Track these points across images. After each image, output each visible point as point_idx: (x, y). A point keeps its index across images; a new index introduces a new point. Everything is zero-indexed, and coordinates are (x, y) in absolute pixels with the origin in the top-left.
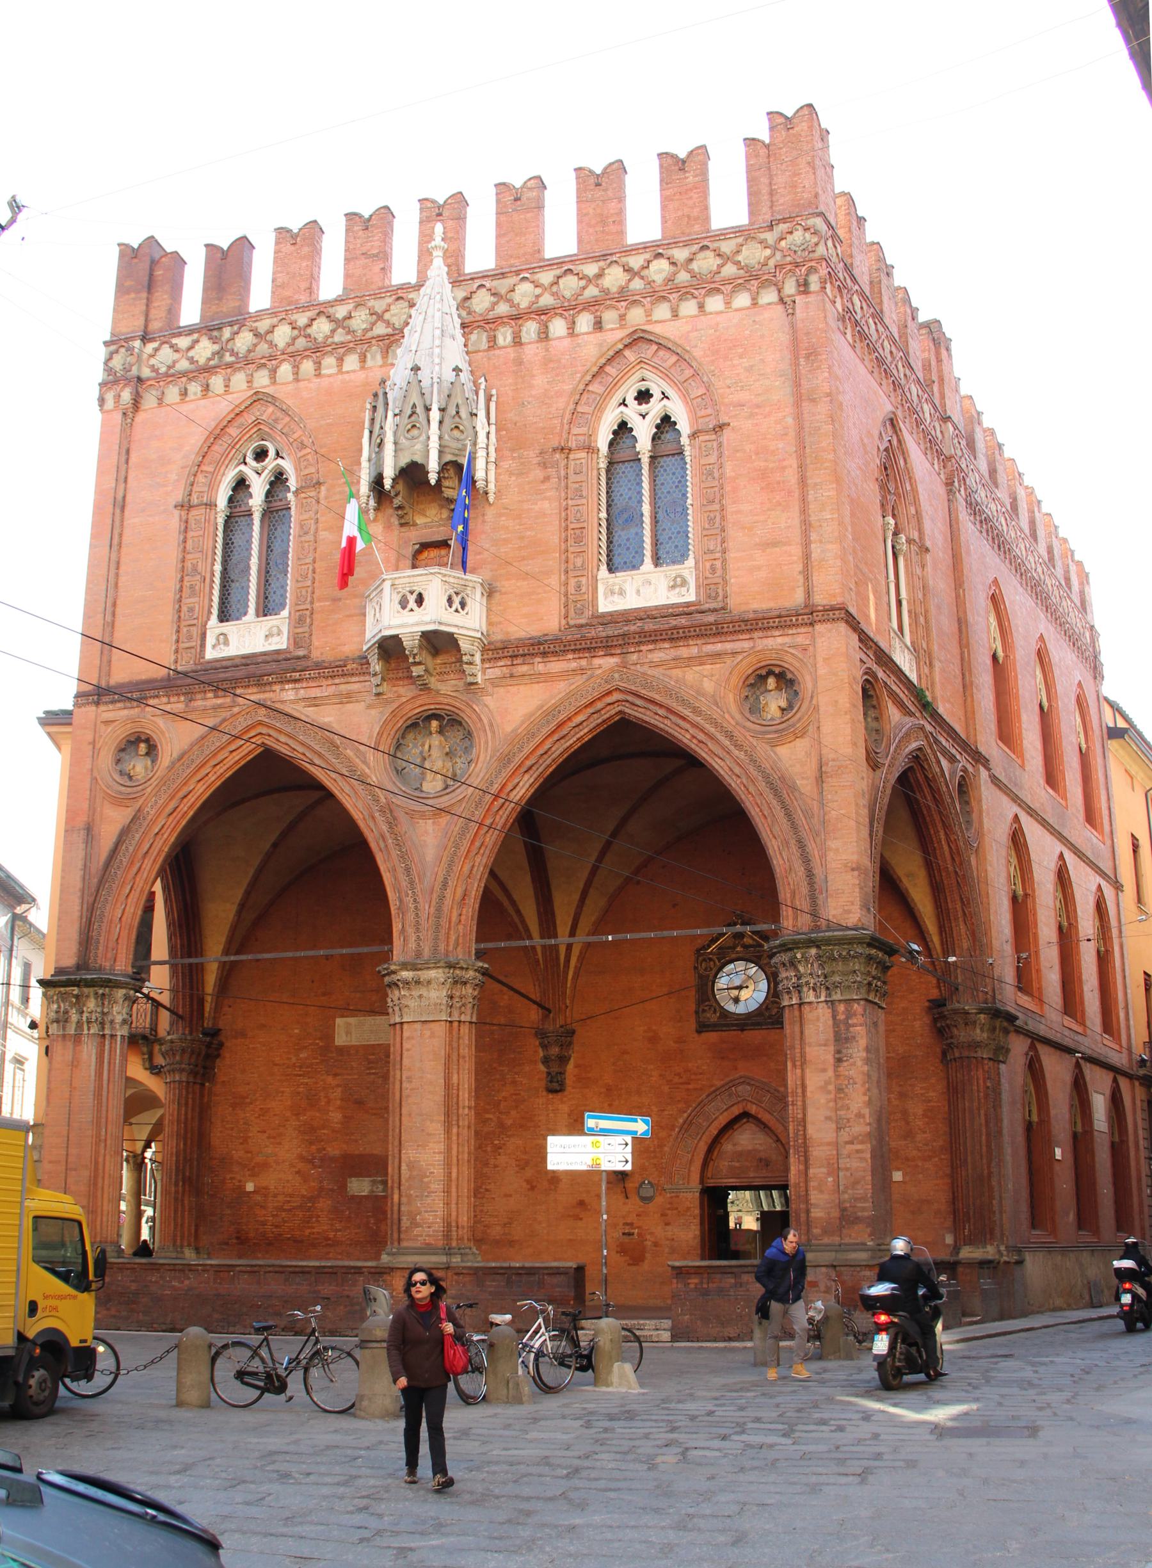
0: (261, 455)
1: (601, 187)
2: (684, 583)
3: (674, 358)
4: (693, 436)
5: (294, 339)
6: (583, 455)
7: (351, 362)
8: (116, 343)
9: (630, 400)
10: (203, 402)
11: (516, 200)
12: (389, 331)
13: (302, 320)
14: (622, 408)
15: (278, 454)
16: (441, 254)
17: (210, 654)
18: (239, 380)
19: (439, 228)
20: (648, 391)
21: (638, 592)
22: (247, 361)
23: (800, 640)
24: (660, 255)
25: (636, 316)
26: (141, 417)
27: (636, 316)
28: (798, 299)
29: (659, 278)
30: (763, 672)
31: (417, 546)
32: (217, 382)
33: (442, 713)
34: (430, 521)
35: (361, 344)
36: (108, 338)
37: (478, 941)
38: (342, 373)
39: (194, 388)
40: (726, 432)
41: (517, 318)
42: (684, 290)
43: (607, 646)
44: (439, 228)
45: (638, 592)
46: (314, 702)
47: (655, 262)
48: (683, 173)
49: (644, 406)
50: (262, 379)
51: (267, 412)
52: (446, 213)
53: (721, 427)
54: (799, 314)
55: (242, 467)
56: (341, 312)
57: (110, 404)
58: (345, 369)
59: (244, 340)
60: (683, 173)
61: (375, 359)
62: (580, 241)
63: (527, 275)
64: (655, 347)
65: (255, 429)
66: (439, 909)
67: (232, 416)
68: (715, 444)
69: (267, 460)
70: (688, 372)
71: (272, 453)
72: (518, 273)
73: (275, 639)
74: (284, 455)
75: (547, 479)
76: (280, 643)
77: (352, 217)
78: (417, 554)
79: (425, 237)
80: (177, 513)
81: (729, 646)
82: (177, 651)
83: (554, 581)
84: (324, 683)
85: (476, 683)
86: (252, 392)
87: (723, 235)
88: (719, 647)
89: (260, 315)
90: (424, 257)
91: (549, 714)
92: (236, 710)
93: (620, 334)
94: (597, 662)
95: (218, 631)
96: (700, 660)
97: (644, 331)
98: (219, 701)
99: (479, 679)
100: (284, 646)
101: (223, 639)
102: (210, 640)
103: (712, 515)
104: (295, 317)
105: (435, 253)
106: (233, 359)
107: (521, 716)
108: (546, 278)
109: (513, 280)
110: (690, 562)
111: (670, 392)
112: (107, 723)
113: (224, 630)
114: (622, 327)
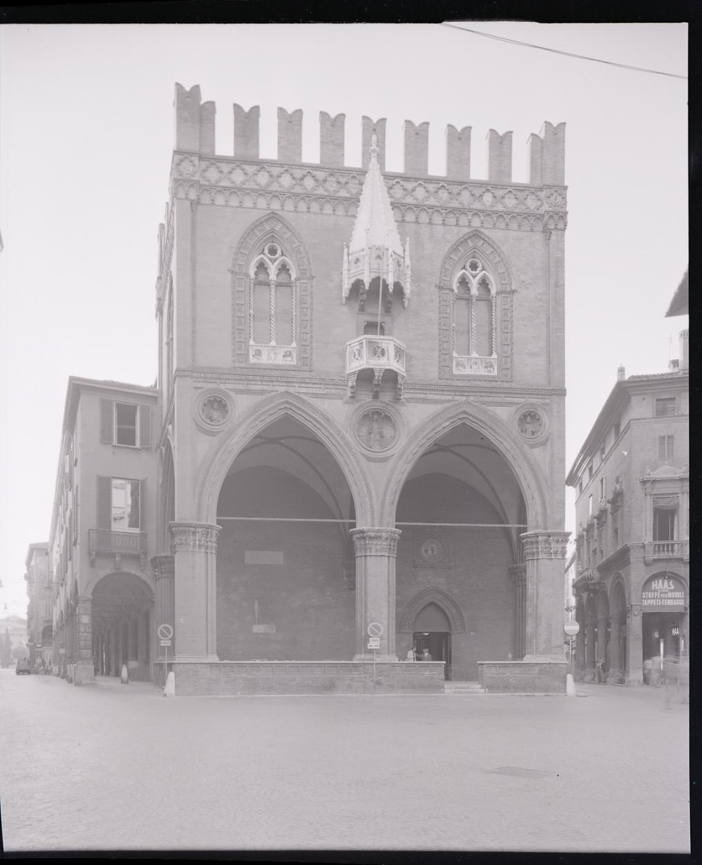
0: (273, 251)
1: (459, 139)
2: (491, 366)
3: (492, 250)
4: (498, 293)
5: (295, 185)
6: (448, 292)
7: (328, 209)
8: (181, 154)
9: (468, 267)
10: (240, 209)
11: (417, 134)
12: (348, 195)
13: (298, 173)
14: (464, 271)
15: (283, 254)
16: (375, 155)
17: (252, 360)
18: (262, 203)
19: (374, 138)
20: (476, 264)
21: (471, 368)
22: (262, 192)
23: (547, 401)
24: (488, 190)
25: (476, 222)
26: (200, 208)
27: (476, 222)
28: (553, 232)
29: (488, 204)
30: (527, 414)
31: (366, 323)
32: (248, 202)
33: (381, 411)
34: (377, 312)
35: (334, 200)
36: (175, 149)
37: (396, 521)
38: (323, 214)
39: (234, 201)
40: (516, 296)
41: (419, 207)
42: (500, 214)
43: (461, 391)
44: (374, 138)
45: (471, 368)
46: (315, 396)
47: (486, 194)
48: (500, 144)
49: (474, 272)
50: (276, 205)
51: (278, 227)
52: (374, 129)
53: (513, 292)
54: (553, 237)
55: (262, 256)
56: (321, 175)
57: (181, 195)
58: (324, 212)
59: (263, 179)
60: (500, 144)
61: (340, 211)
62: (449, 170)
63: (422, 183)
64: (482, 242)
65: (270, 235)
66: (383, 505)
67: (258, 223)
68: (509, 300)
69: (277, 256)
70: (498, 259)
71: (279, 252)
72: (417, 179)
73: (289, 359)
74: (287, 255)
75: (432, 301)
76: (292, 361)
77: (324, 115)
78: (366, 327)
79: (366, 143)
80: (229, 275)
81: (515, 400)
82: (234, 356)
83: (436, 354)
84: (323, 387)
85: (400, 399)
86: (268, 212)
87: (521, 188)
88: (509, 399)
89: (272, 163)
90: (366, 155)
91: (434, 418)
92: (273, 393)
93: (467, 230)
94: (456, 398)
95: (255, 348)
96: (501, 404)
97: (480, 232)
98: (262, 387)
99: (402, 397)
100: (295, 363)
101: (258, 353)
102: (251, 353)
103: (506, 335)
104: (294, 171)
105: (373, 154)
106: (256, 187)
107: (418, 420)
108: (431, 187)
109: (415, 184)
110: (494, 356)
111: (486, 266)
112: (196, 388)
113: (260, 348)
114: (470, 226)
